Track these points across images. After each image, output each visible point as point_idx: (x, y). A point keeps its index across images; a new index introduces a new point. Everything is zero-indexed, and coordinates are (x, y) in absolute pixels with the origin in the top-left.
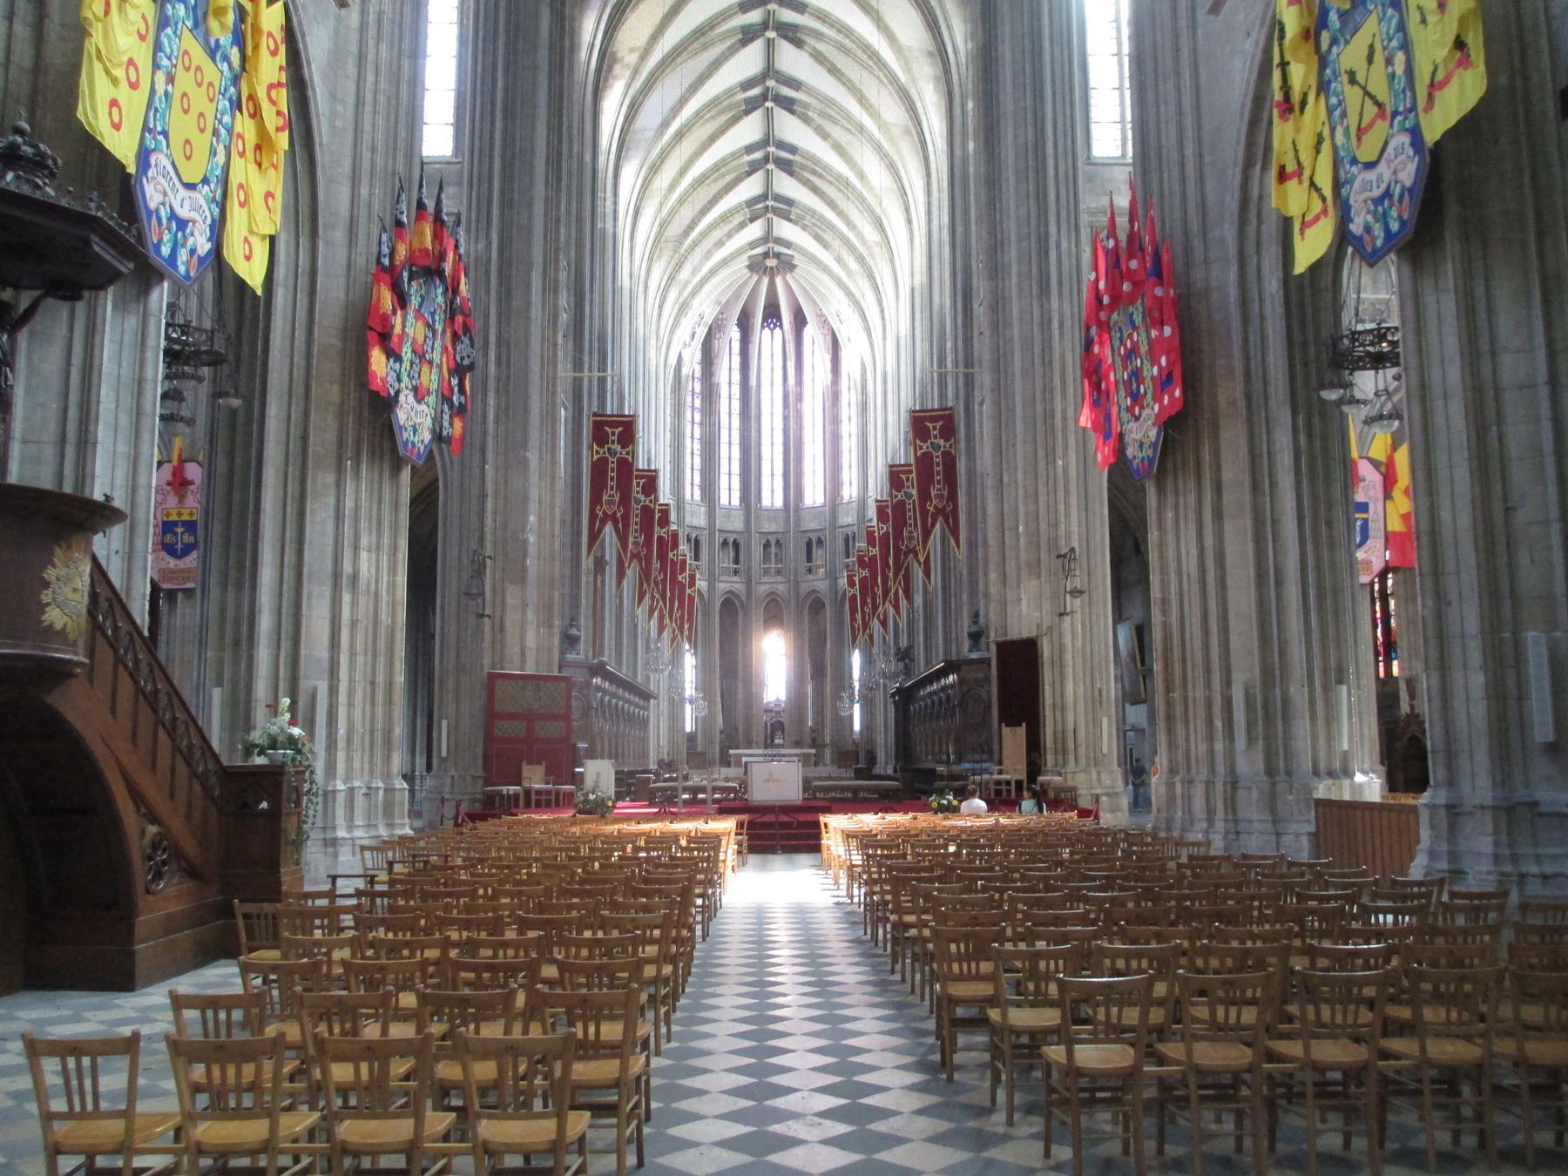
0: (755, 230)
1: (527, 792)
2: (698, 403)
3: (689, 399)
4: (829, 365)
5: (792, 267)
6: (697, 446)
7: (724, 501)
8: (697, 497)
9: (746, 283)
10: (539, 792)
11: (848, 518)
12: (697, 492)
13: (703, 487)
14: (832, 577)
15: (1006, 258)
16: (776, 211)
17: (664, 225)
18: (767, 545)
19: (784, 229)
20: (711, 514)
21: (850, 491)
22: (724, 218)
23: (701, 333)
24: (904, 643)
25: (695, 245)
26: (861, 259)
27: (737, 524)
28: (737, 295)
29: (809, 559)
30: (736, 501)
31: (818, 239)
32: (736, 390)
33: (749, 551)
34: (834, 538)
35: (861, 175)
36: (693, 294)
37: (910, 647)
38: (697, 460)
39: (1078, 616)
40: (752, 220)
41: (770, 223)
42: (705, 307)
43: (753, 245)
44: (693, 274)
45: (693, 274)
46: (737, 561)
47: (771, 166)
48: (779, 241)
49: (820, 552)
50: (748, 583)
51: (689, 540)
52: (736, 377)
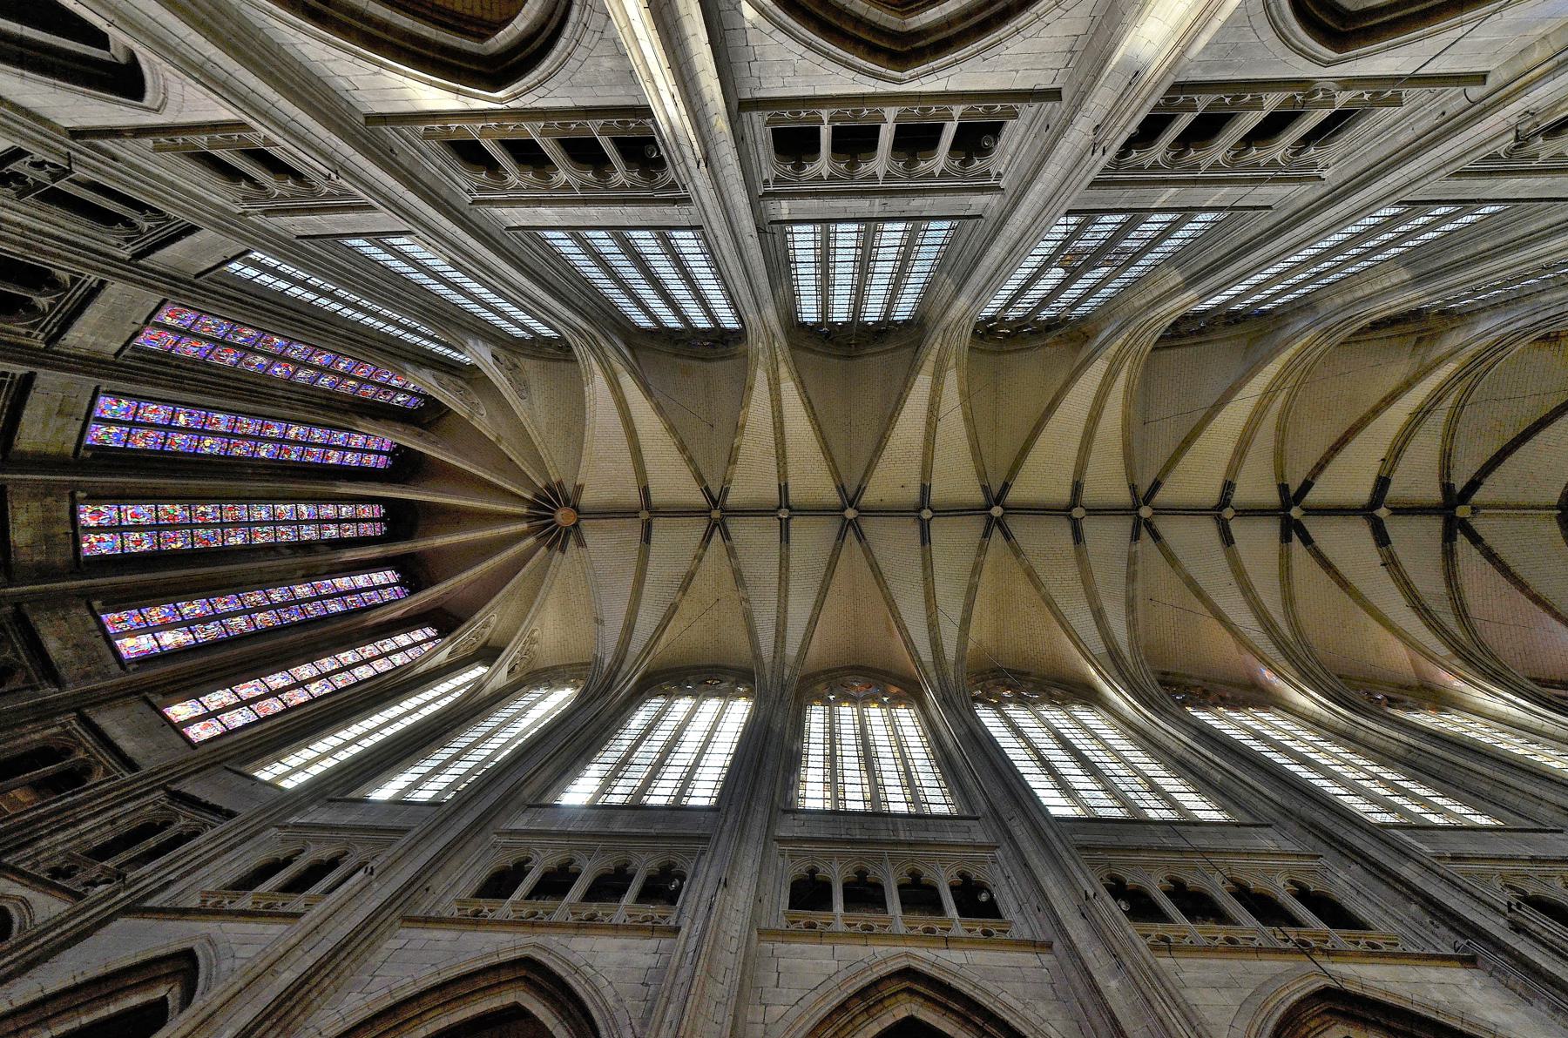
7: (108, 407)
20: (88, 363)
30: (102, 435)
32: (314, 456)
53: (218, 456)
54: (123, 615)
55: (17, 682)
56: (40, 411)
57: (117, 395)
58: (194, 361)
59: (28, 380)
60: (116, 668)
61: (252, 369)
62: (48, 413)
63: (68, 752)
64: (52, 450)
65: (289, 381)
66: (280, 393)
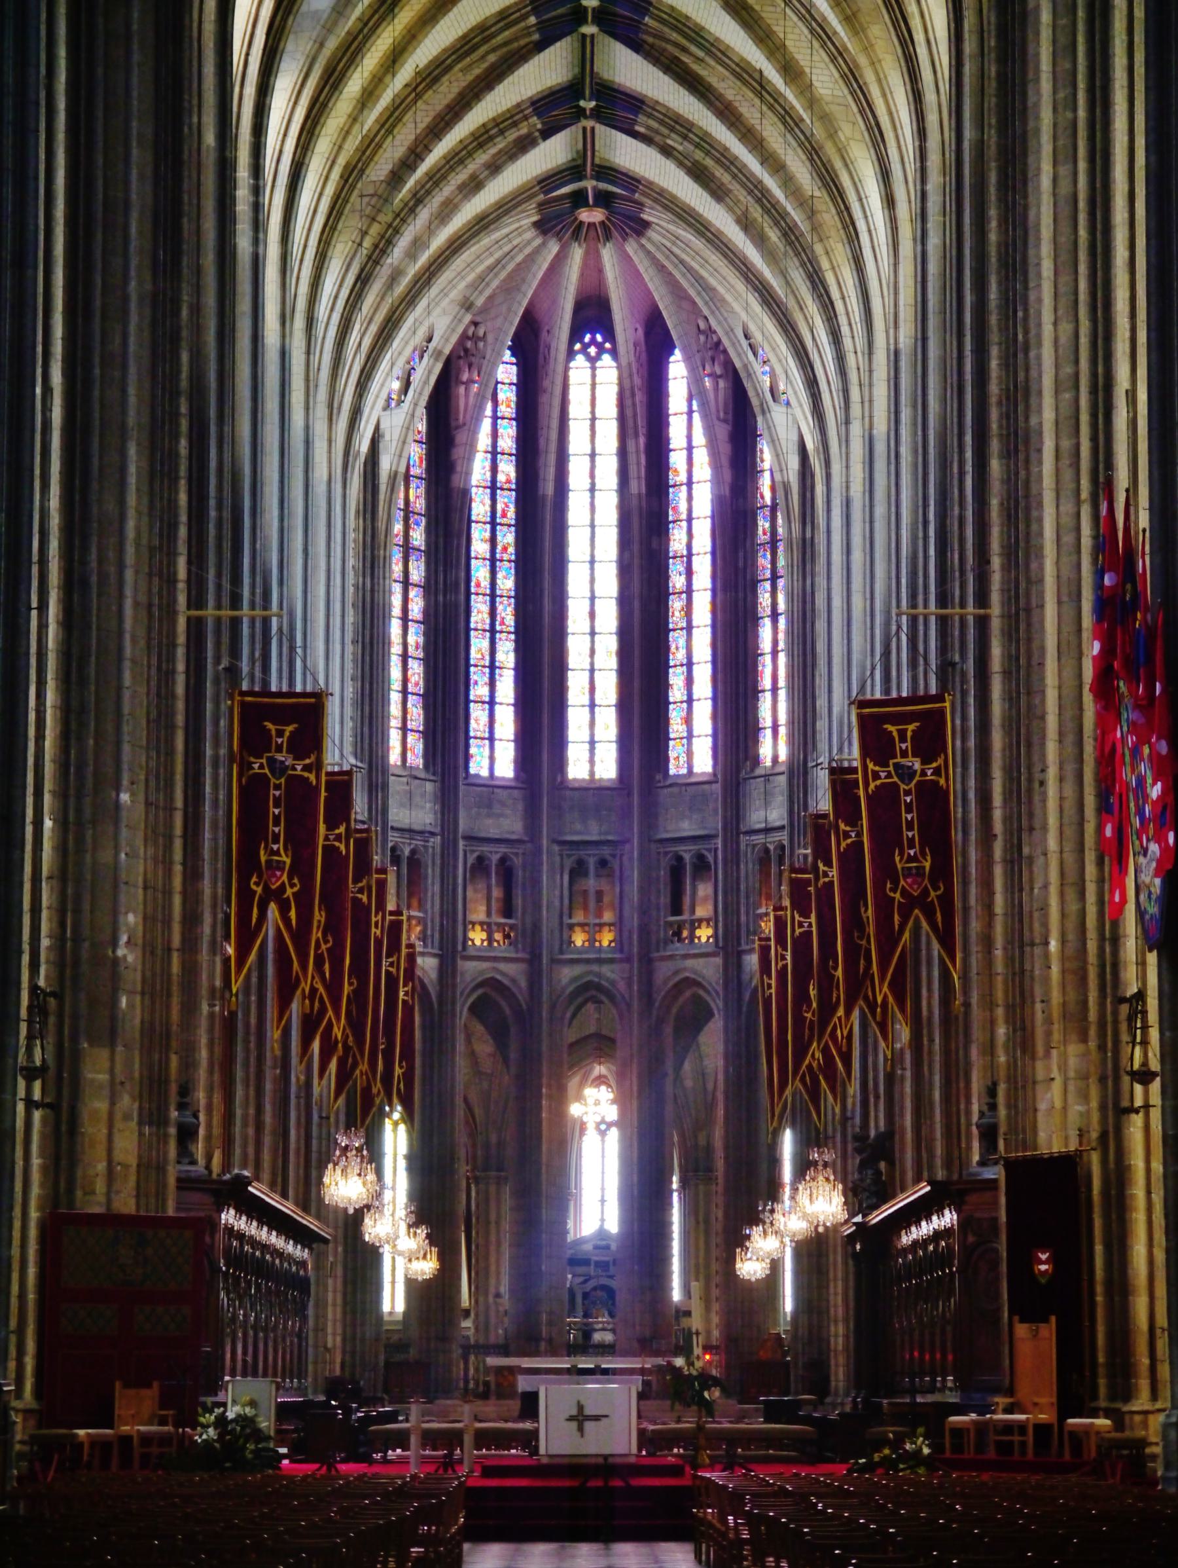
0: (552, 153)
1: (126, 1440)
2: (418, 537)
3: (398, 527)
4: (725, 448)
5: (640, 227)
6: (415, 637)
7: (479, 766)
8: (416, 759)
9: (531, 259)
10: (146, 1439)
11: (769, 812)
12: (416, 744)
13: (430, 734)
14: (729, 946)
15: (1033, 421)
16: (597, 114)
17: (353, 174)
18: (578, 871)
19: (627, 153)
21: (773, 748)
22: (482, 138)
23: (426, 374)
24: (878, 1124)
25: (418, 198)
26: (790, 233)
27: (510, 824)
28: (511, 286)
29: (677, 909)
31: (699, 174)
32: (507, 502)
33: (536, 882)
34: (733, 856)
35: (790, 70)
36: (410, 299)
37: (889, 1137)
38: (416, 670)
39: (1156, 1115)
40: (547, 134)
41: (588, 138)
42: (436, 320)
43: (548, 181)
44: (411, 255)
45: (411, 255)
46: (508, 911)
47: (589, 29)
48: (606, 172)
49: (704, 889)
50: (533, 961)
51: (396, 859)
52: (508, 470)
53: (516, 641)
54: (672, 754)
55: (710, 859)
56: (490, 821)
57: (467, 757)
58: (426, 708)
59: (469, 838)
60: (714, 786)
61: (421, 640)
62: (489, 816)
63: (767, 851)
64: (520, 806)
65: (429, 588)
66: (441, 598)
